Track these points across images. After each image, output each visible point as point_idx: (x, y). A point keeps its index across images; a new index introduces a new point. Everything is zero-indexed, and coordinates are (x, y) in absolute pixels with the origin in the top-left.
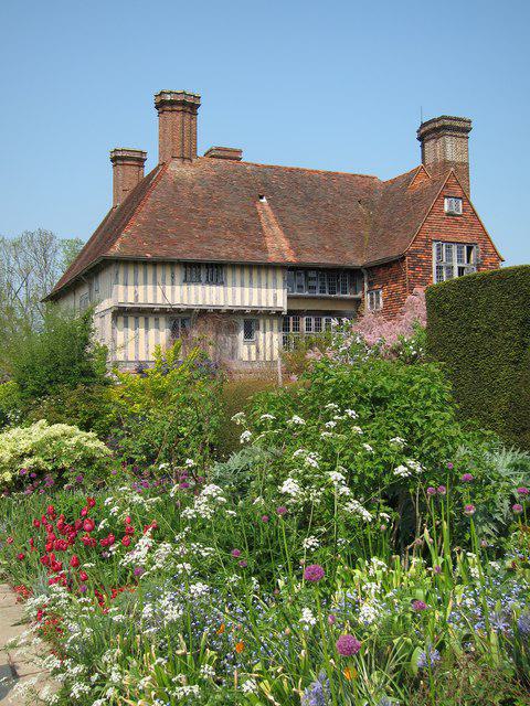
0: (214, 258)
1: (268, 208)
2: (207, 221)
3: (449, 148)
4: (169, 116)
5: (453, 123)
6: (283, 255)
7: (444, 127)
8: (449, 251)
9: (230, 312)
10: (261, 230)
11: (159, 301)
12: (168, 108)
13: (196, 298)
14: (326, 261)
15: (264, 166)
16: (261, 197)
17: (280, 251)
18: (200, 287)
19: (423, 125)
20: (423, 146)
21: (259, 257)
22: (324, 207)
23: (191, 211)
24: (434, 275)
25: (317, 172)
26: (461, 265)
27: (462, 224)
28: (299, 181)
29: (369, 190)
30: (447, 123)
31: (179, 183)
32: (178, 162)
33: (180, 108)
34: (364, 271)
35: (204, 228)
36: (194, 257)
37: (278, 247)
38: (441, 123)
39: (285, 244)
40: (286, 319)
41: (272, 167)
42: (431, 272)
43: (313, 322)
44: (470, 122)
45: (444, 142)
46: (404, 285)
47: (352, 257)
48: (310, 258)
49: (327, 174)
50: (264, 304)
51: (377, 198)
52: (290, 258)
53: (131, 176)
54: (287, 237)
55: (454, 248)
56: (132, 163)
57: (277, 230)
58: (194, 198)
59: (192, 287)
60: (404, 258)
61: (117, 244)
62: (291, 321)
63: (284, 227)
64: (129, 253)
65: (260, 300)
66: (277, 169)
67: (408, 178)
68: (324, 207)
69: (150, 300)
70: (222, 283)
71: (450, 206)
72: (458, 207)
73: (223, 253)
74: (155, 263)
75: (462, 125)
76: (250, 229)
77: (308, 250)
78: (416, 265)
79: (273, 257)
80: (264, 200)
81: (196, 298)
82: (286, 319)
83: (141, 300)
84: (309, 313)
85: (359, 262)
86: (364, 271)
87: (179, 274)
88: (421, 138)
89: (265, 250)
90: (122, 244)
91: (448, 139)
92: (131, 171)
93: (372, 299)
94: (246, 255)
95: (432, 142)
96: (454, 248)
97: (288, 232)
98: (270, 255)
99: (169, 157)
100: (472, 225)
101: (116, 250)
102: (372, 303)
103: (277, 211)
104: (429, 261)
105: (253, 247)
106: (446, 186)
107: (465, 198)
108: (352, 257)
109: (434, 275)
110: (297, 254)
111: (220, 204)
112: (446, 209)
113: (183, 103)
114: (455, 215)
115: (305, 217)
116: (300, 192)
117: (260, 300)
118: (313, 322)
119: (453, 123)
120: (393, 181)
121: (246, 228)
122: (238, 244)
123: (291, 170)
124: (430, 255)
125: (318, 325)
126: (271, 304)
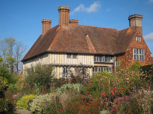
0: (75, 52)
1: (89, 38)
2: (73, 41)
3: (138, 23)
4: (62, 13)
5: (138, 16)
6: (93, 51)
7: (135, 17)
8: (137, 51)
9: (79, 66)
10: (87, 44)
11: (61, 63)
12: (62, 10)
13: (70, 62)
14: (104, 53)
15: (87, 26)
16: (87, 35)
17: (92, 50)
18: (71, 59)
19: (130, 16)
20: (130, 22)
21: (87, 51)
22: (103, 38)
23: (68, 39)
24: (134, 57)
25: (101, 28)
27: (141, 44)
28: (97, 31)
29: (115, 33)
30: (136, 16)
31: (64, 32)
32: (64, 25)
33: (65, 10)
34: (114, 55)
35: (72, 43)
36: (69, 51)
37: (92, 48)
38: (135, 16)
39: (93, 48)
40: (94, 68)
41: (89, 27)
42: (133, 56)
43: (101, 69)
45: (136, 21)
46: (126, 60)
47: (111, 52)
48: (100, 52)
49: (104, 29)
50: (88, 64)
51: (117, 35)
52: (95, 52)
53: (47, 28)
54: (94, 46)
55: (139, 50)
56: (48, 23)
57: (91, 44)
58: (69, 35)
59: (69, 59)
60: (126, 52)
61: (50, 48)
62: (95, 69)
63: (93, 43)
64: (53, 50)
65: (87, 63)
66: (91, 27)
67: (126, 30)
68: (103, 38)
69: (58, 63)
70: (77, 58)
72: (140, 39)
73: (77, 50)
74: (60, 53)
75: (140, 16)
76: (84, 44)
77: (100, 50)
79: (91, 52)
80: (87, 36)
81: (70, 62)
82: (94, 68)
83: (56, 63)
84: (100, 66)
85: (113, 53)
86: (114, 55)
87: (66, 56)
88: (129, 19)
89: (88, 50)
90: (51, 48)
91: (137, 20)
92: (48, 25)
93: (117, 63)
94: (84, 51)
95: (132, 21)
96: (139, 50)
97: (94, 45)
98: (90, 51)
99: (62, 23)
100: (143, 44)
101: (49, 49)
102: (117, 64)
103: (91, 38)
104: (132, 54)
105: (85, 49)
106: (137, 34)
107: (141, 37)
108: (111, 52)
109: (134, 57)
110: (97, 51)
111: (76, 37)
112: (137, 40)
113: (66, 9)
114: (139, 41)
115: (98, 40)
116: (96, 33)
117: (87, 63)
118: (101, 69)
119: (138, 16)
120: (122, 31)
121: (83, 43)
122: (81, 48)
123: (94, 27)
124: (132, 52)
125: (102, 70)
126: (90, 64)
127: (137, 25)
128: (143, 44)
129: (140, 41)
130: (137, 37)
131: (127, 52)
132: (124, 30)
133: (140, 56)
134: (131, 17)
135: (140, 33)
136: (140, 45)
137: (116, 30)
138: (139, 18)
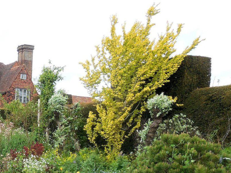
19: (19, 47)
26: (25, 96)
27: (26, 83)
44: (34, 46)
60: (6, 93)
67: (12, 65)
71: (22, 77)
78: (10, 96)
88: (18, 51)
100: (29, 83)
106: (22, 70)
127: (26, 59)
128: (29, 83)
129: (26, 79)
130: (21, 75)
131: (8, 92)
132: (10, 64)
133: (25, 98)
134: (20, 48)
135: (25, 69)
136: (24, 84)
137: (2, 63)
138: (30, 49)
